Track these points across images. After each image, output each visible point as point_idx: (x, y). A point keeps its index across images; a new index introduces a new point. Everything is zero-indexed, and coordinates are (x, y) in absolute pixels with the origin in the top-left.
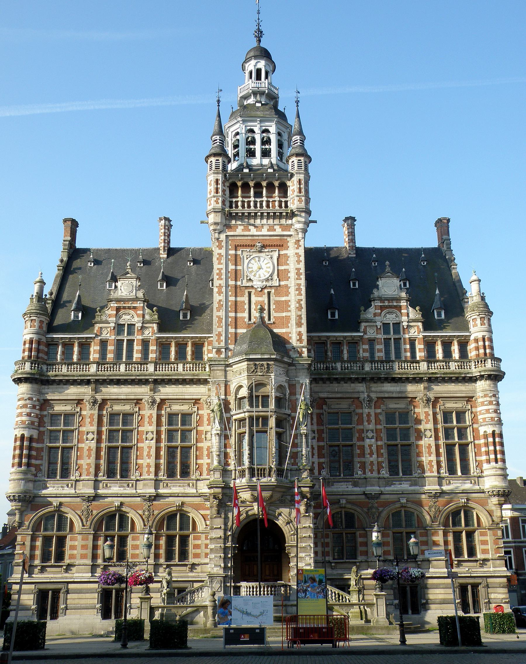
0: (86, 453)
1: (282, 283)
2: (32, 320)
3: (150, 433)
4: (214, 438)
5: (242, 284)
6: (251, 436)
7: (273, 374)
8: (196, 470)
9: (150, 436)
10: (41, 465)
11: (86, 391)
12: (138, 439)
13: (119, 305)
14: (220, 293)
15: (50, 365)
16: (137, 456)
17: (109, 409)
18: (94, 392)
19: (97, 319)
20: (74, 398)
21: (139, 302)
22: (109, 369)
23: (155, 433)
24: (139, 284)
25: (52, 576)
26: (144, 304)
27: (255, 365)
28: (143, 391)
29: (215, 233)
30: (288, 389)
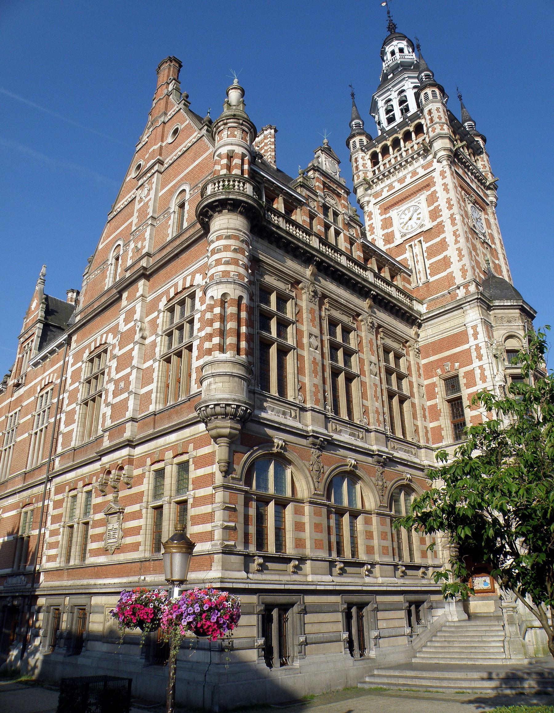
2: (243, 130)
3: (373, 364)
17: (328, 313)
18: (313, 278)
21: (343, 191)
25: (276, 577)
28: (364, 304)
29: (448, 160)
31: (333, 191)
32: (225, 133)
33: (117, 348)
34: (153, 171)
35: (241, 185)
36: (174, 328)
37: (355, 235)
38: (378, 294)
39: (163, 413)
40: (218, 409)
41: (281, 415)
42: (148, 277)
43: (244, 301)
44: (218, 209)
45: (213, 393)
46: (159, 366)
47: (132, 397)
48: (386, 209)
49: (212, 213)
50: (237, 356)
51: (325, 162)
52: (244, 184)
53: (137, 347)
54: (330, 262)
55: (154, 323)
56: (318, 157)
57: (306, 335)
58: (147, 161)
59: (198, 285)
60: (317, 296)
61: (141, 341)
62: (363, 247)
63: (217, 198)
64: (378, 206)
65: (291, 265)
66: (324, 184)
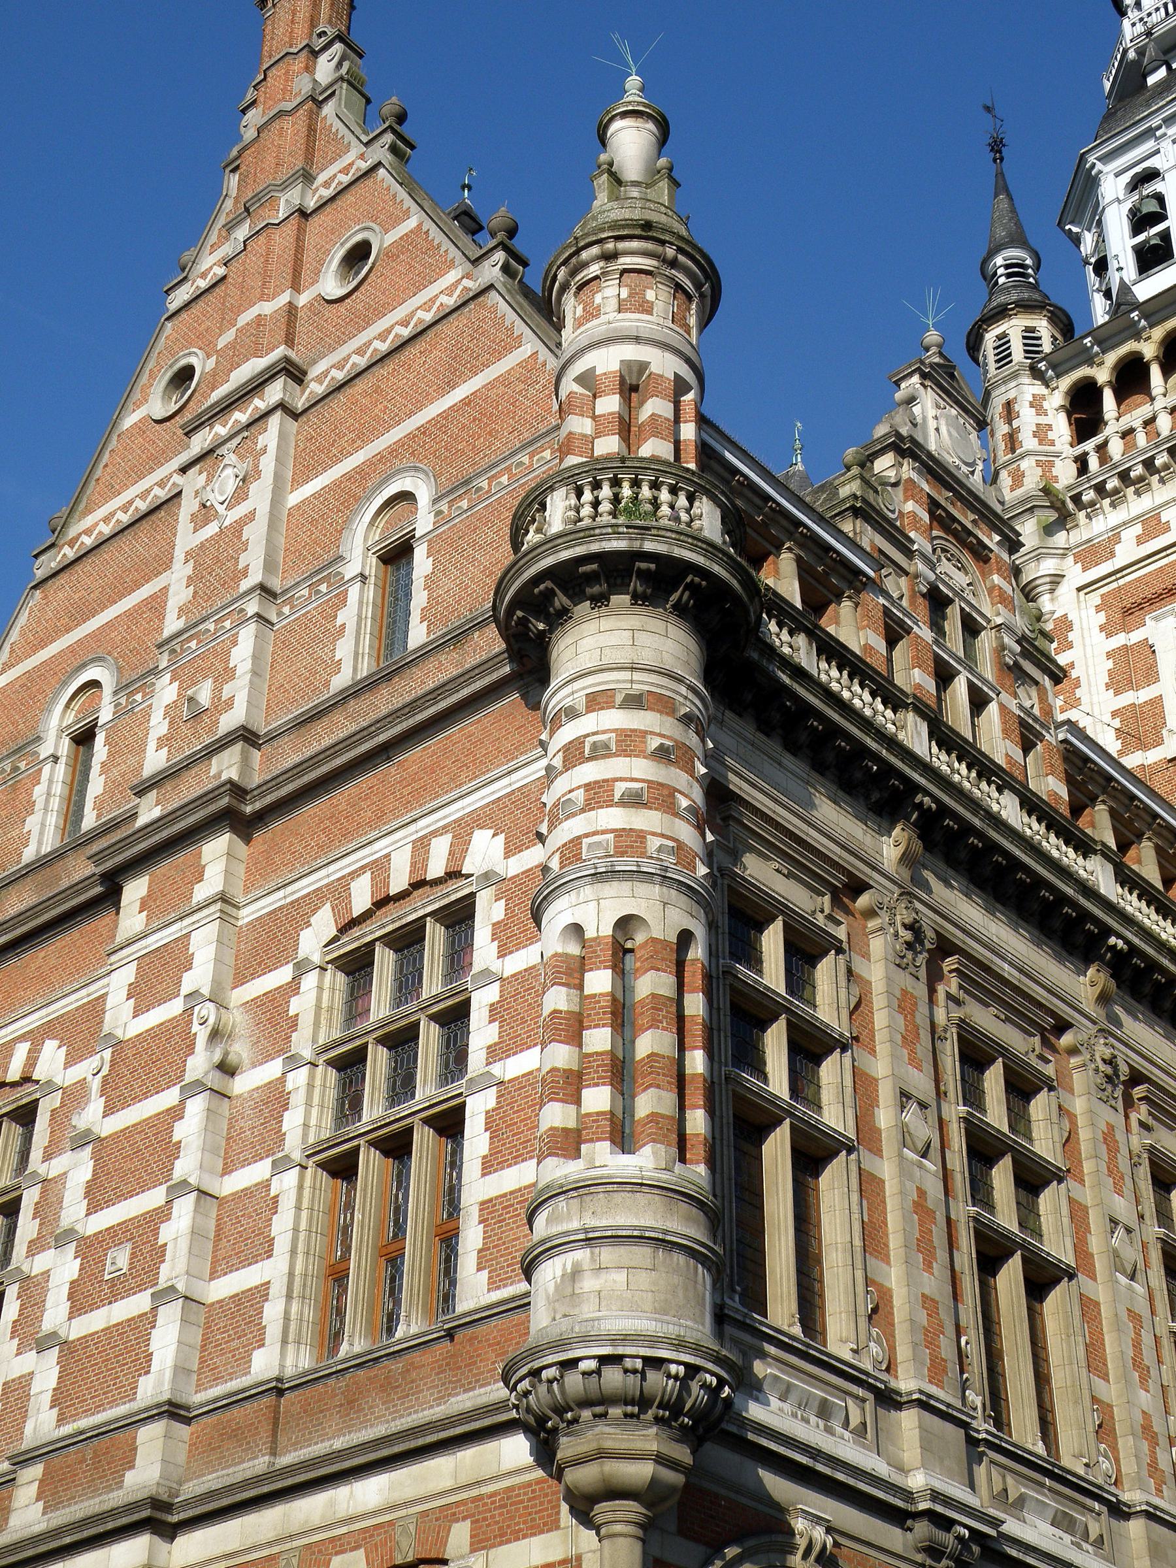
2: (678, 287)
18: (905, 874)
21: (997, 538)
28: (1083, 985)
31: (963, 537)
32: (609, 293)
33: (96, 1105)
34: (259, 404)
35: (682, 501)
36: (370, 1039)
37: (1036, 711)
38: (1133, 950)
39: (320, 1387)
40: (613, 1377)
41: (813, 1419)
42: (245, 826)
43: (697, 952)
44: (596, 589)
45: (588, 1310)
46: (301, 1187)
47: (170, 1314)
48: (1129, 609)
49: (566, 601)
50: (678, 1167)
51: (936, 422)
52: (691, 498)
53: (196, 1106)
54: (968, 815)
55: (274, 1015)
56: (911, 400)
57: (886, 1094)
58: (234, 356)
59: (487, 876)
60: (922, 944)
61: (215, 1079)
62: (1066, 759)
63: (595, 547)
64: (1095, 598)
65: (833, 821)
66: (933, 505)
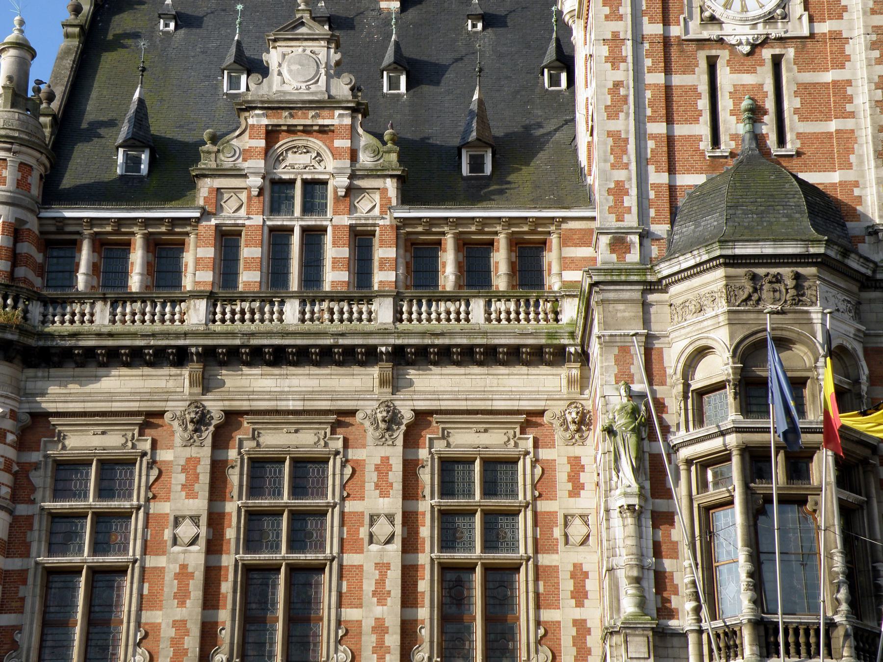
0: (170, 585)
1: (822, 28)
3: (383, 520)
4: (616, 520)
5: (687, 32)
6: (757, 510)
7: (818, 308)
8: (538, 642)
9: (382, 529)
10: (19, 628)
11: (171, 386)
12: (342, 541)
13: (275, 121)
14: (615, 60)
15: (54, 302)
16: (340, 595)
17: (249, 445)
18: (198, 390)
19: (207, 163)
20: (134, 406)
21: (337, 112)
22: (247, 316)
23: (398, 519)
24: (338, 56)
26: (353, 118)
27: (754, 278)
28: (359, 385)
30: (864, 363)
